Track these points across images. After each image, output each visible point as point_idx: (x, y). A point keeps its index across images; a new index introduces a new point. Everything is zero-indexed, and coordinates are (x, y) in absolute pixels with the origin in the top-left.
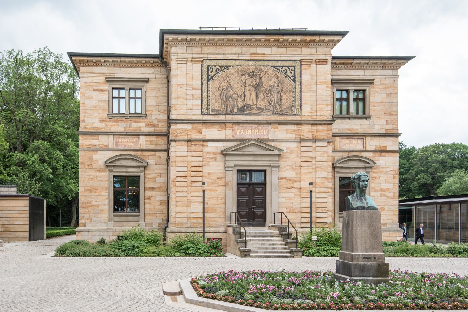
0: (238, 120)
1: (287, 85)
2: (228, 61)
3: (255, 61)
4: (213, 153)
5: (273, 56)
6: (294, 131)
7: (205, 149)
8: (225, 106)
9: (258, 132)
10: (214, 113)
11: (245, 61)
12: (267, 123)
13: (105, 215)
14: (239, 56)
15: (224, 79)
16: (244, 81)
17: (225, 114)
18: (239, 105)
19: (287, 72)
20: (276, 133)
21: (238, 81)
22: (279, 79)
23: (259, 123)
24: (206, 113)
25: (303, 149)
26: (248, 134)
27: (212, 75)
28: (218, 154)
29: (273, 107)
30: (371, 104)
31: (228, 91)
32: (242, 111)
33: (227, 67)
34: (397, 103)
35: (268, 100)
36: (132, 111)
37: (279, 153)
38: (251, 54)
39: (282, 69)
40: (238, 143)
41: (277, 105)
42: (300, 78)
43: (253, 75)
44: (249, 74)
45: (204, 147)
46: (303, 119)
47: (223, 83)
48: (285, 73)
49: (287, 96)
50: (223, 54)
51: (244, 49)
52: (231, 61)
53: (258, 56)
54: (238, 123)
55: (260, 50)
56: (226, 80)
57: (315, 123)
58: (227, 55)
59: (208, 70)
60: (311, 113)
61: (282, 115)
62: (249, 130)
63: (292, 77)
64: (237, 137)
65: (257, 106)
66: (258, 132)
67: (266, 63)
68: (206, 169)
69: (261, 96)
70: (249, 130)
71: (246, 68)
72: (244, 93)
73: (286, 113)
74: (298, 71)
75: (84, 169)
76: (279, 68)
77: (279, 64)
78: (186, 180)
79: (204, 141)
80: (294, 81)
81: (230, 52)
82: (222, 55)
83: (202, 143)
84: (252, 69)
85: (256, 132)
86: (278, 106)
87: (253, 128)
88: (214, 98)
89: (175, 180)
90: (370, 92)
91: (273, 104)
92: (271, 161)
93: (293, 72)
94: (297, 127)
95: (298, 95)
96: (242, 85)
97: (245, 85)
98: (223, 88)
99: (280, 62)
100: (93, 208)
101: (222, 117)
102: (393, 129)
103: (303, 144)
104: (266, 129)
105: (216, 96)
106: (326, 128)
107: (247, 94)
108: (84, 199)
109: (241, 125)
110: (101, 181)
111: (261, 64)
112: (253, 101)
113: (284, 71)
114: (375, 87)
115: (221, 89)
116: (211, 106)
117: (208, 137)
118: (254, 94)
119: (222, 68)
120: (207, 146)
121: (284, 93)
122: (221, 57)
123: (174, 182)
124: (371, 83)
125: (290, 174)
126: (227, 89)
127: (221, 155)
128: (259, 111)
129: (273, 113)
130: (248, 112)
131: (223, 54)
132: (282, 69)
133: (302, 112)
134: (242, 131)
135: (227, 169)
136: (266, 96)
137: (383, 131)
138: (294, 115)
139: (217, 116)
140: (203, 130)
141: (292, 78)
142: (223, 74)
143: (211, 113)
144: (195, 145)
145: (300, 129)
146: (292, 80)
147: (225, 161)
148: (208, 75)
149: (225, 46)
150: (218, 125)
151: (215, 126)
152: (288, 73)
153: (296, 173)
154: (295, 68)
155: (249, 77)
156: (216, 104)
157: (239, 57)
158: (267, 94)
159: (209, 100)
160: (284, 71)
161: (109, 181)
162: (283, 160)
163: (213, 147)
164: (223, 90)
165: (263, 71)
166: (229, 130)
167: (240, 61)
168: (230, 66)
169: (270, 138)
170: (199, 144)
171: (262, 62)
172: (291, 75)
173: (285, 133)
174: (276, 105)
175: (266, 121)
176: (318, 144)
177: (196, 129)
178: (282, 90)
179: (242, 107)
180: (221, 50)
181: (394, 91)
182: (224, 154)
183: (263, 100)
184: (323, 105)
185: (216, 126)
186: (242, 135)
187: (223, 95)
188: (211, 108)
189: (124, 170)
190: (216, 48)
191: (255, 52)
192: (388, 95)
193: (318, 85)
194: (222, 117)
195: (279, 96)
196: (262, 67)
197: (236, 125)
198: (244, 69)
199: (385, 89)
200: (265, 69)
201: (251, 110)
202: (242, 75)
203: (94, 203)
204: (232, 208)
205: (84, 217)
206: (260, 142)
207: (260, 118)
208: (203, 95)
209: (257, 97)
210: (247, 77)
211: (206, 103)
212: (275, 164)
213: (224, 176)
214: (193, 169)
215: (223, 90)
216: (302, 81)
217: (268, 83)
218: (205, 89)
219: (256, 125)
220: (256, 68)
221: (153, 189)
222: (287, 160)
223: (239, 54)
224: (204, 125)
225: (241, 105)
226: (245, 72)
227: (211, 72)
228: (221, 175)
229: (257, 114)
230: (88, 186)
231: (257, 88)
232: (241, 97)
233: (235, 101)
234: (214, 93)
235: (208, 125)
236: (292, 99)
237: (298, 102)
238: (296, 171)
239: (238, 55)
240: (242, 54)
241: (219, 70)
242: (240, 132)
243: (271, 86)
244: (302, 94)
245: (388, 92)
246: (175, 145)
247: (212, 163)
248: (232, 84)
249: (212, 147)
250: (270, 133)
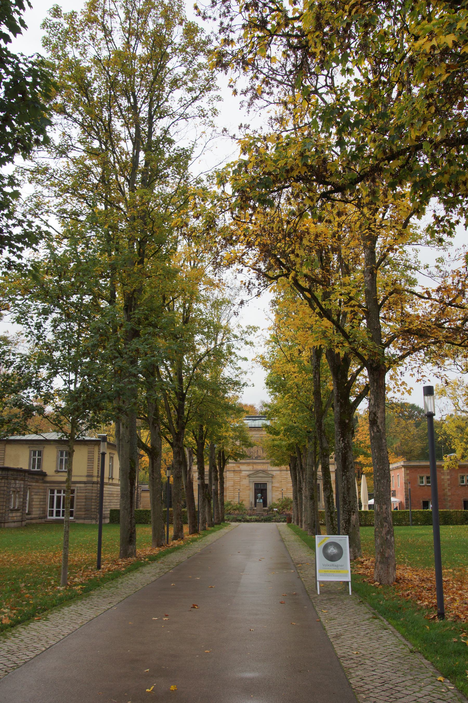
7: (241, 474)
32: (256, 458)
68: (242, 483)
79: (240, 471)
125: (276, 485)
182: (249, 476)
207: (264, 461)
247: (244, 480)
249: (244, 473)
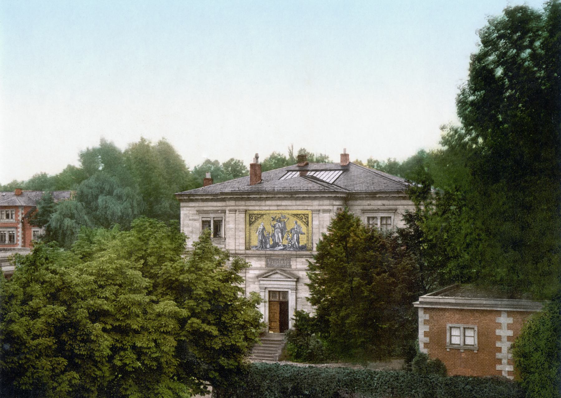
43: (280, 221)
69: (285, 236)
80: (308, 225)
81: (264, 204)
84: (279, 216)
118: (280, 235)
148: (250, 221)
168: (264, 214)
172: (305, 221)
209: (283, 237)
231: (282, 231)
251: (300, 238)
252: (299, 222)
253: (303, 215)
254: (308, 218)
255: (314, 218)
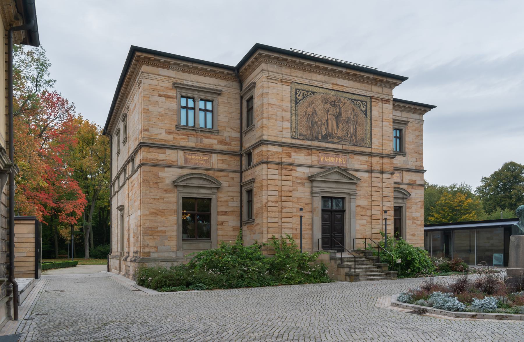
0: (323, 147)
1: (361, 118)
2: (314, 87)
3: (336, 92)
4: (301, 178)
5: (351, 89)
6: (367, 162)
7: (294, 174)
8: (311, 132)
9: (339, 160)
10: (301, 138)
11: (328, 90)
12: (346, 153)
13: (174, 243)
14: (323, 84)
15: (310, 104)
16: (327, 109)
17: (311, 140)
18: (323, 132)
19: (360, 106)
20: (353, 162)
21: (322, 109)
22: (355, 111)
23: (339, 152)
24: (295, 137)
25: (374, 180)
26: (330, 162)
27: (300, 99)
28: (305, 179)
29: (350, 137)
30: (406, 142)
31: (313, 117)
32: (325, 138)
33: (313, 93)
34: (423, 143)
35: (346, 131)
36: (202, 125)
37: (356, 182)
38: (333, 84)
39: (357, 102)
40: (325, 170)
41: (353, 136)
42: (370, 113)
43: (334, 104)
44: (330, 103)
45: (293, 171)
46: (373, 151)
47: (309, 108)
48: (359, 107)
49: (361, 129)
50: (310, 80)
51: (327, 78)
52: (316, 87)
53: (339, 86)
54: (322, 150)
55: (340, 81)
56: (311, 106)
57: (382, 156)
58: (313, 82)
59: (296, 93)
60: (379, 146)
61: (357, 146)
62: (331, 158)
63: (365, 111)
64: (321, 163)
65: (338, 136)
66: (339, 160)
67: (345, 95)
70: (331, 158)
71: (329, 97)
72: (327, 120)
73: (360, 144)
74: (369, 106)
75: (149, 187)
76: (355, 102)
77: (354, 97)
78: (277, 205)
80: (366, 115)
81: (315, 79)
82: (309, 81)
83: (291, 167)
84: (333, 99)
85: (337, 160)
86: (354, 137)
87: (335, 156)
88: (301, 122)
89: (266, 205)
90: (405, 132)
91: (350, 134)
92: (350, 189)
93: (365, 107)
94: (369, 159)
95: (369, 129)
96: (325, 113)
97: (327, 114)
98: (309, 113)
99: (355, 95)
100: (159, 234)
101: (309, 143)
102: (420, 166)
103: (374, 175)
104: (345, 158)
105: (303, 121)
106: (389, 162)
107: (330, 122)
108: (148, 224)
109: (325, 152)
110: (169, 203)
111: (340, 95)
112: (334, 130)
113: (358, 104)
114: (409, 128)
115: (308, 114)
116: (299, 130)
117: (297, 162)
118: (334, 123)
119: (309, 94)
120: (296, 170)
121: (359, 126)
122: (307, 82)
123: (266, 206)
124: (406, 124)
126: (312, 115)
127: (307, 181)
128: (339, 140)
129: (350, 143)
130: (330, 140)
131: (310, 80)
132: (357, 102)
133: (372, 145)
134: (326, 158)
135: (314, 195)
136: (344, 126)
137: (414, 167)
138: (366, 147)
139: (304, 141)
140: (293, 154)
141: (365, 112)
142: (309, 99)
143: (299, 137)
144: (286, 169)
145: (371, 160)
146: (364, 113)
147: (312, 187)
148: (296, 98)
149: (312, 72)
150: (306, 150)
151: (303, 151)
152: (362, 107)
153: (368, 201)
154: (366, 104)
155: (331, 106)
156: (303, 129)
157: (323, 85)
158: (345, 125)
159: (297, 124)
160: (358, 104)
161: (177, 203)
162: (358, 188)
163: (301, 172)
164: (309, 115)
165: (342, 102)
166: (315, 156)
167: (324, 89)
168: (315, 93)
169: (348, 167)
170: (289, 168)
171: (341, 93)
173: (360, 163)
174: (352, 136)
175: (346, 150)
176: (385, 176)
177: (286, 153)
178: (357, 122)
179: (325, 134)
180: (308, 75)
181: (421, 133)
182: (311, 179)
183: (342, 130)
184: (387, 140)
185: (304, 151)
186: (326, 162)
187: (309, 120)
188: (299, 133)
189: (195, 191)
190: (303, 72)
191: (335, 83)
192: (417, 136)
193: (384, 121)
194: (309, 143)
195: (355, 127)
196: (341, 98)
197: (321, 152)
198: (326, 97)
199: (415, 130)
200: (344, 100)
201: (333, 138)
202: (325, 103)
203: (160, 229)
204: (318, 235)
205: (148, 245)
206: (343, 170)
207: (340, 147)
208: (292, 118)
209: (338, 127)
210: (329, 106)
211: (295, 127)
212: (353, 192)
213: (311, 202)
214: (284, 194)
215: (309, 115)
216: (372, 116)
217: (346, 114)
218: (293, 112)
219: (337, 154)
220: (336, 98)
221: (225, 213)
222: (361, 189)
223: (323, 82)
224: (293, 149)
225: (324, 132)
226: (328, 100)
227: (299, 96)
228: (308, 201)
229: (337, 142)
230: (153, 209)
231: (338, 117)
232: (324, 124)
233: (320, 128)
234: (301, 118)
235: (296, 150)
236: (365, 132)
237: (369, 136)
238: (368, 200)
239: (322, 83)
240: (325, 82)
241: (305, 95)
242: (324, 159)
243: (349, 117)
244: (372, 128)
245: (417, 134)
246: (267, 168)
247: (300, 189)
248: (317, 111)
250: (348, 162)
251: (358, 130)
252: (357, 110)
253: (361, 101)
254: (366, 106)
255: (373, 107)
